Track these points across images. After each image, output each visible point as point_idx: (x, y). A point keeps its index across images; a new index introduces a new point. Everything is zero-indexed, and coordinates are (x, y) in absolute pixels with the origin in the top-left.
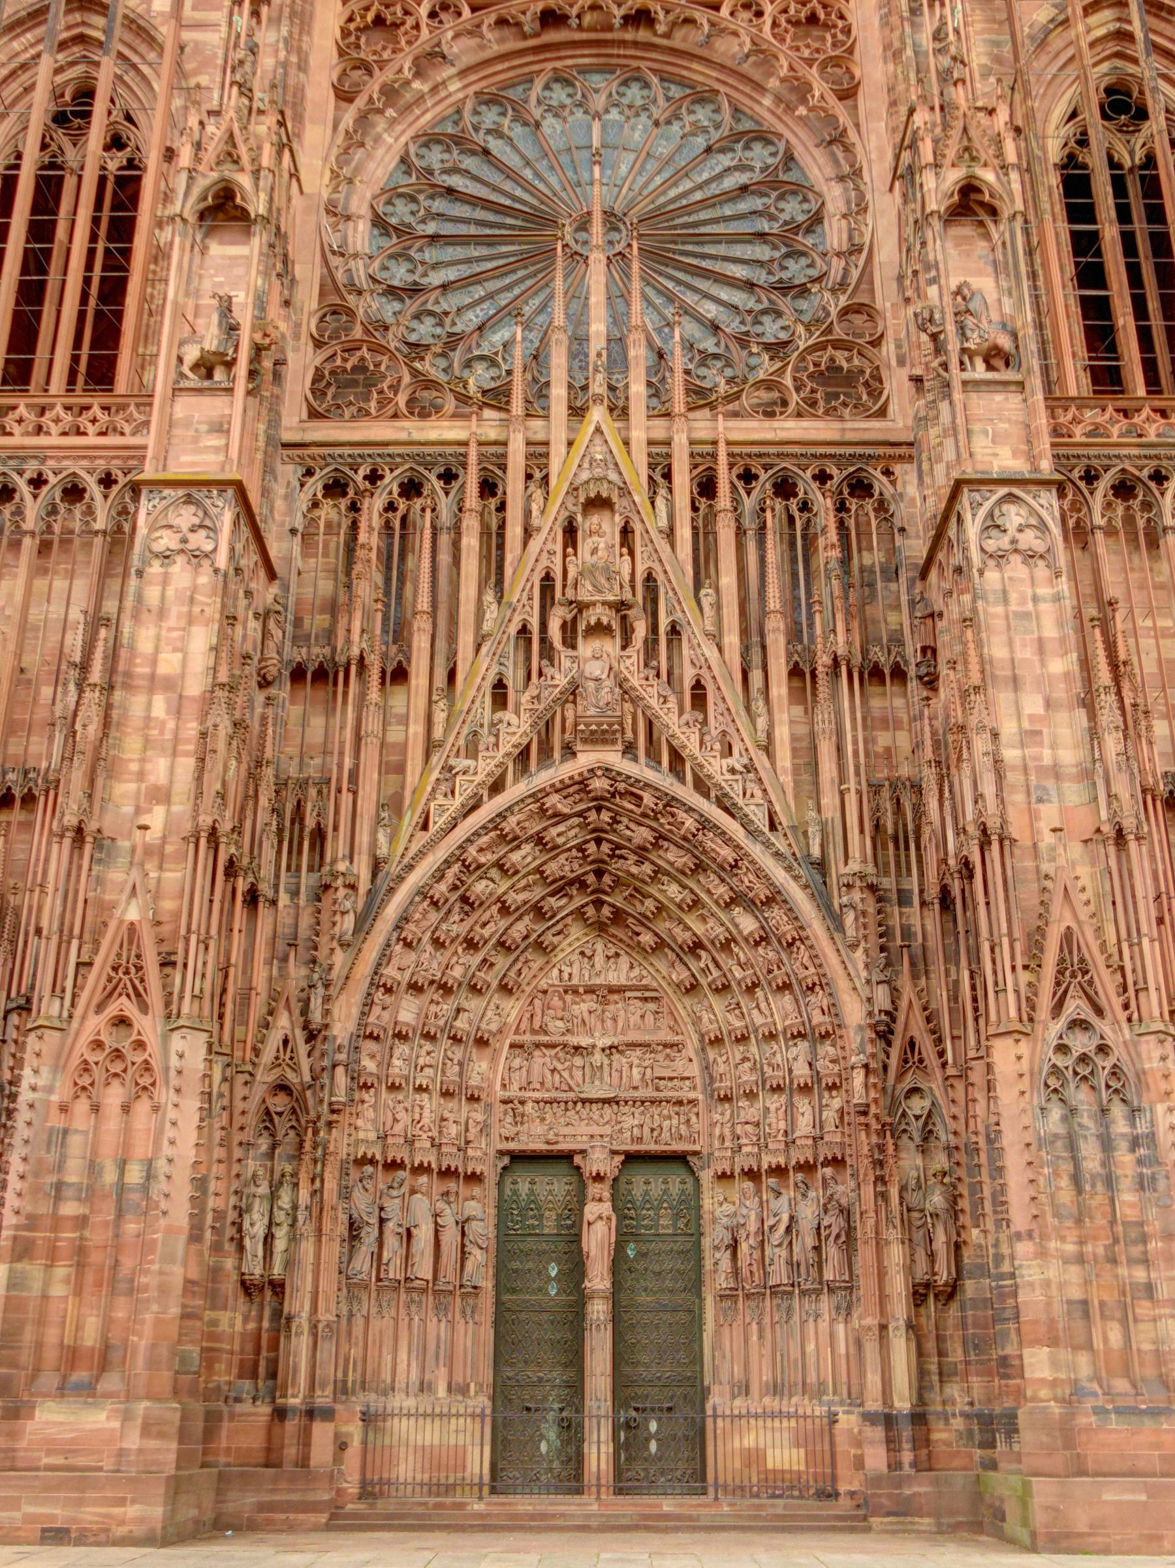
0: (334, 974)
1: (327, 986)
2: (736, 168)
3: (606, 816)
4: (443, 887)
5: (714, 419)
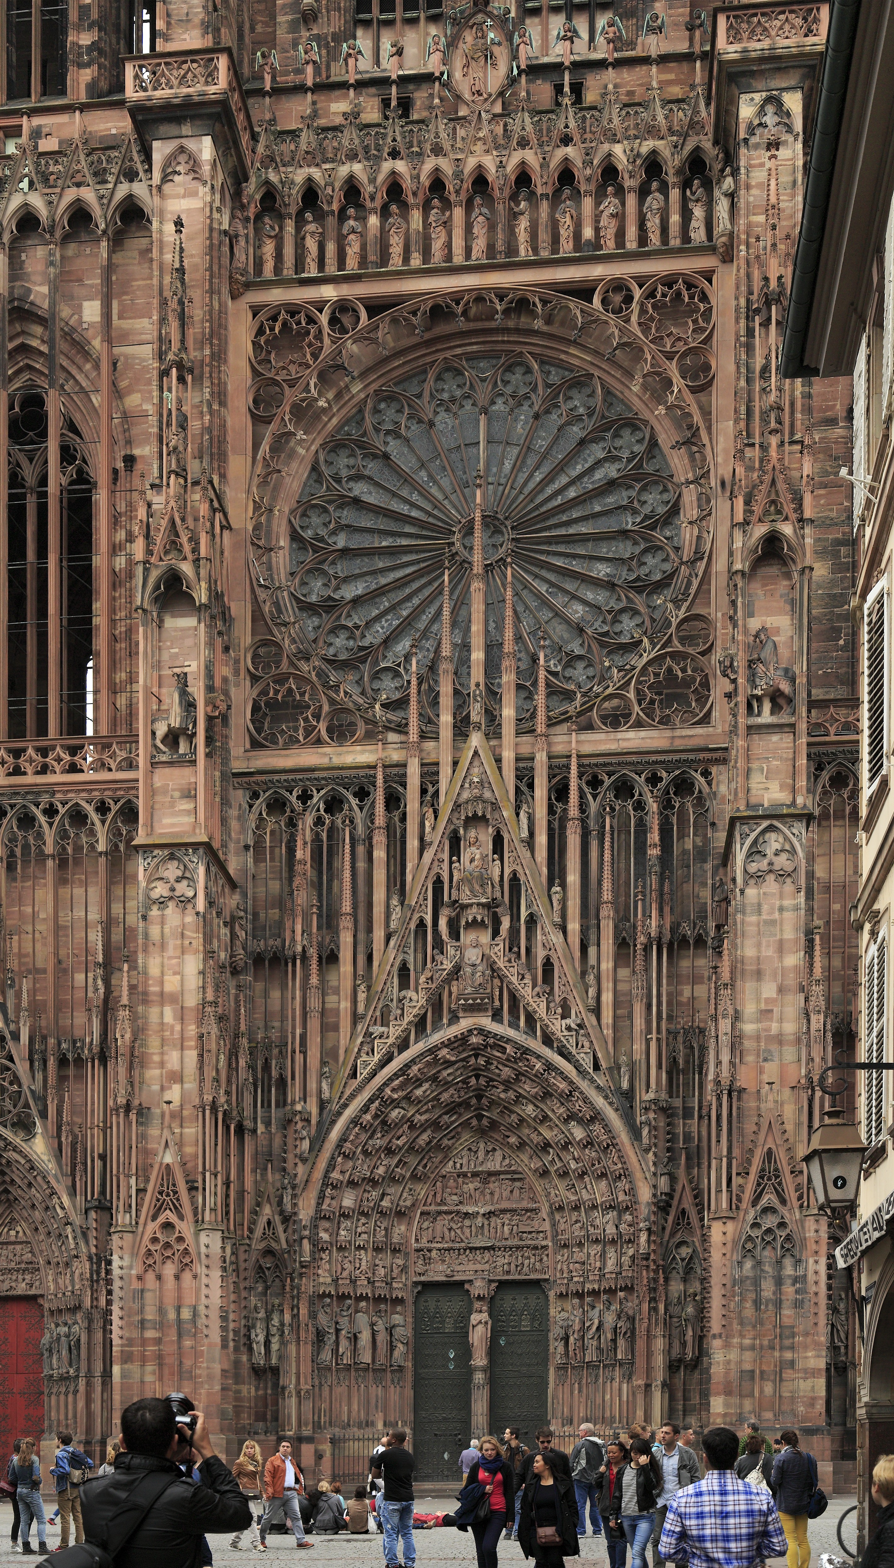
0: (297, 1181)
1: (294, 1187)
2: (605, 459)
3: (481, 1061)
4: (368, 1117)
5: (570, 731)
